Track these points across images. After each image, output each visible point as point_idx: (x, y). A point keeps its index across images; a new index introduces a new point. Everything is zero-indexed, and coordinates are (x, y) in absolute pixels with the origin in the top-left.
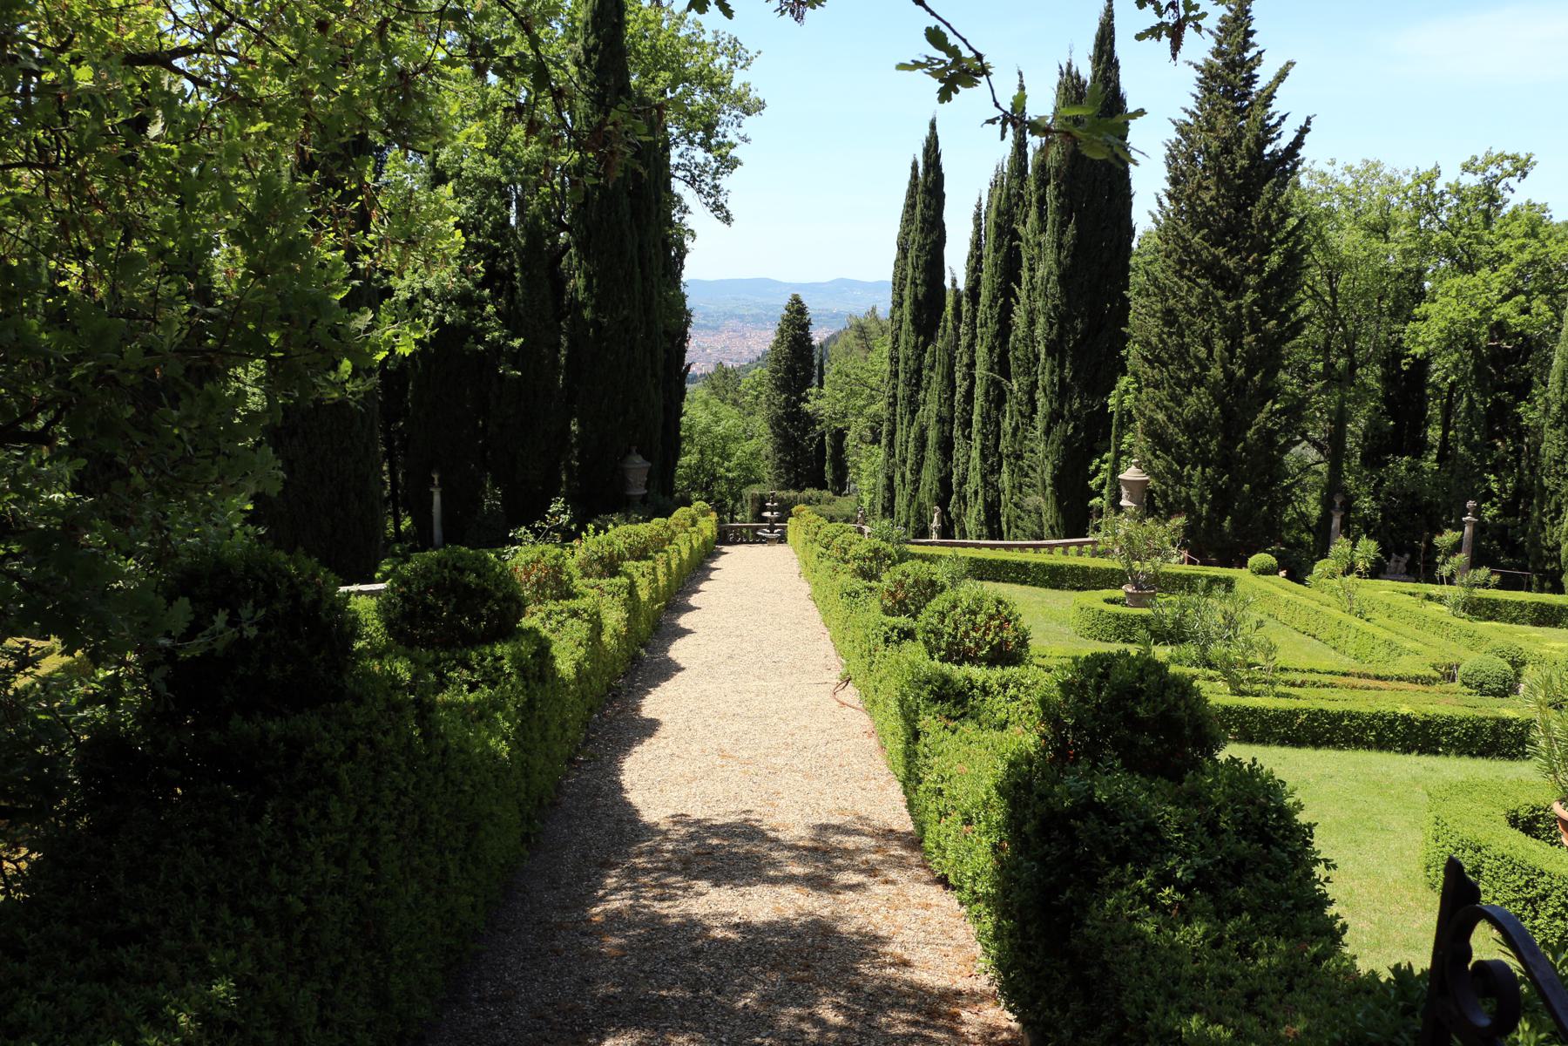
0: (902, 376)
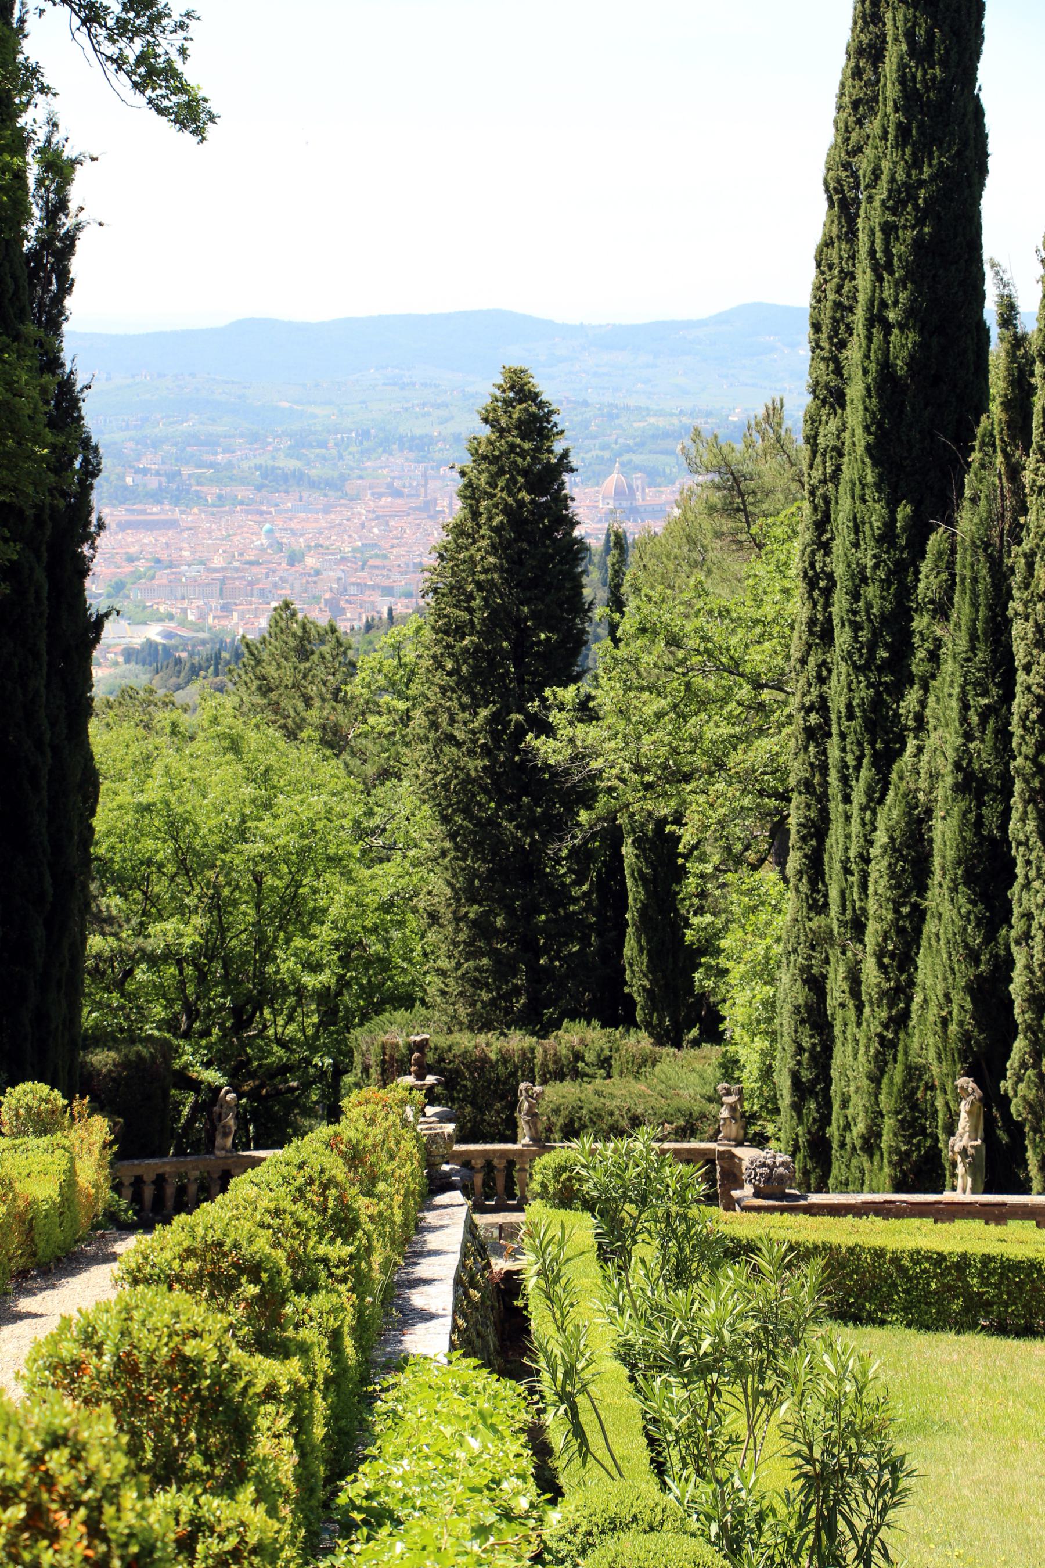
0: (842, 637)
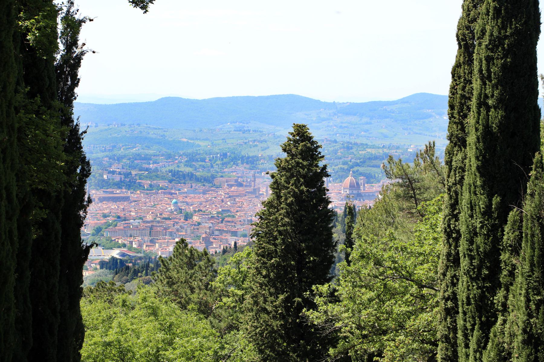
0: (464, 263)
